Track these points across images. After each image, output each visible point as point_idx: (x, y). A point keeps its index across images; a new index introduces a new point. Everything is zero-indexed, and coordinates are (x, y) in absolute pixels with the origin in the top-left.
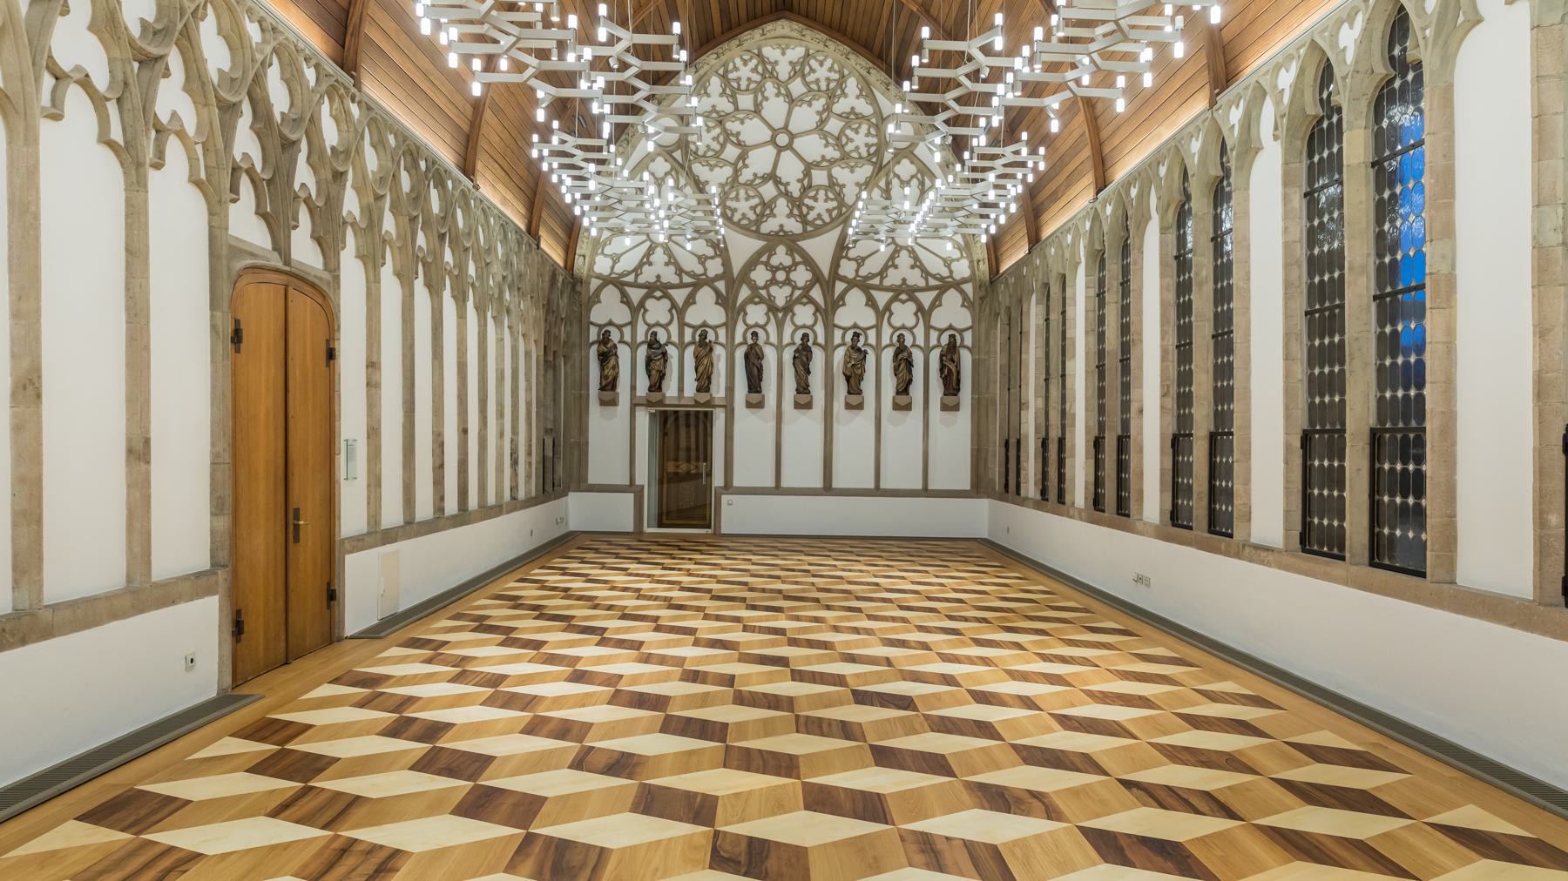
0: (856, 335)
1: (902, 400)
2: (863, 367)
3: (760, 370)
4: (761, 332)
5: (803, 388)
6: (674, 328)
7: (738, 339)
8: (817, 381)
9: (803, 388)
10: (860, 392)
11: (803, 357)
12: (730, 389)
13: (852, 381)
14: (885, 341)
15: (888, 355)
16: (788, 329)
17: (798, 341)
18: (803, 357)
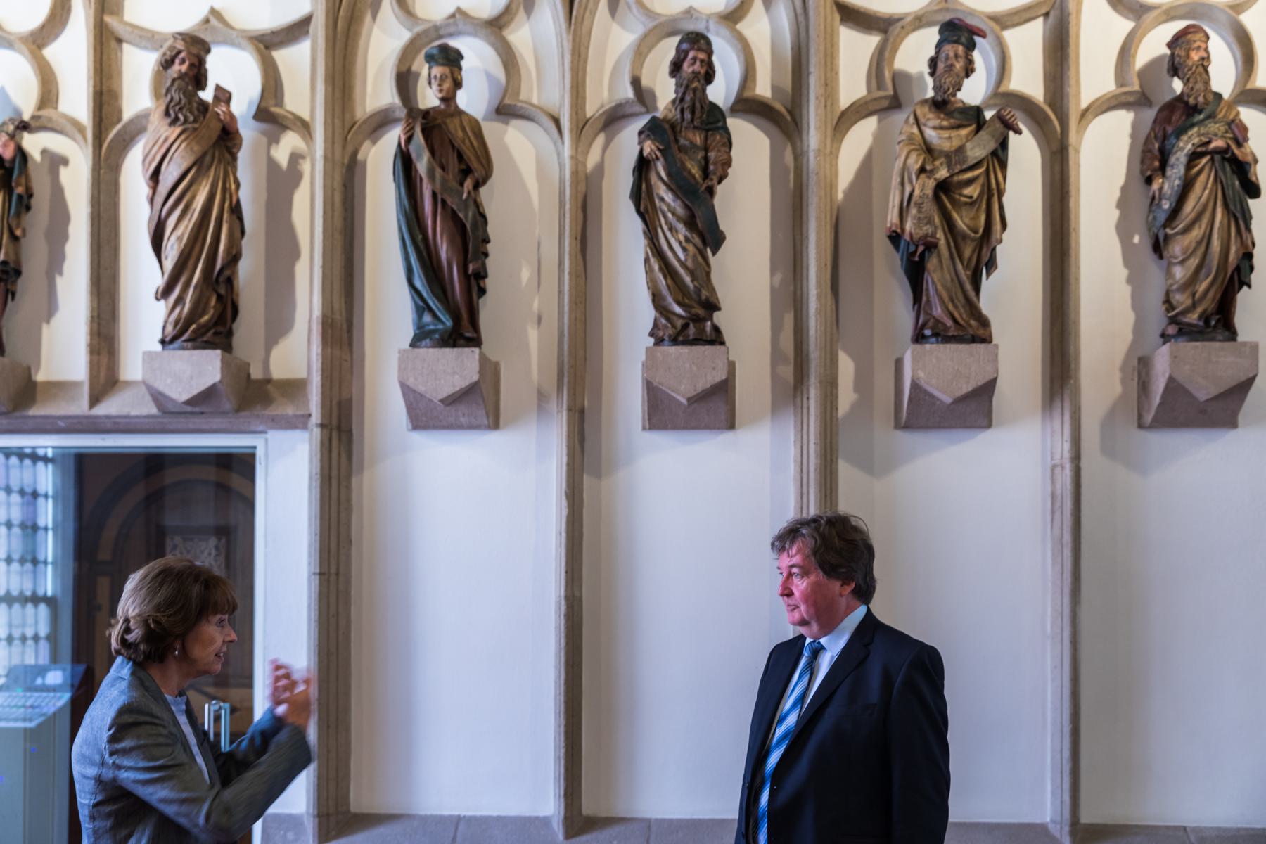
0: (959, 34)
1: (1204, 365)
2: (993, 194)
3: (471, 237)
4: (477, 56)
5: (690, 315)
6: (72, 54)
7: (378, 93)
8: (744, 272)
9: (690, 315)
10: (972, 329)
11: (683, 151)
12: (342, 330)
13: (937, 275)
14: (1094, 76)
15: (1105, 150)
16: (615, 40)
17: (665, 92)
18: (683, 151)
